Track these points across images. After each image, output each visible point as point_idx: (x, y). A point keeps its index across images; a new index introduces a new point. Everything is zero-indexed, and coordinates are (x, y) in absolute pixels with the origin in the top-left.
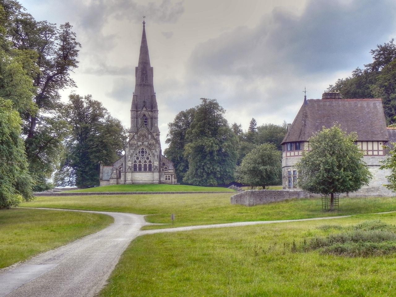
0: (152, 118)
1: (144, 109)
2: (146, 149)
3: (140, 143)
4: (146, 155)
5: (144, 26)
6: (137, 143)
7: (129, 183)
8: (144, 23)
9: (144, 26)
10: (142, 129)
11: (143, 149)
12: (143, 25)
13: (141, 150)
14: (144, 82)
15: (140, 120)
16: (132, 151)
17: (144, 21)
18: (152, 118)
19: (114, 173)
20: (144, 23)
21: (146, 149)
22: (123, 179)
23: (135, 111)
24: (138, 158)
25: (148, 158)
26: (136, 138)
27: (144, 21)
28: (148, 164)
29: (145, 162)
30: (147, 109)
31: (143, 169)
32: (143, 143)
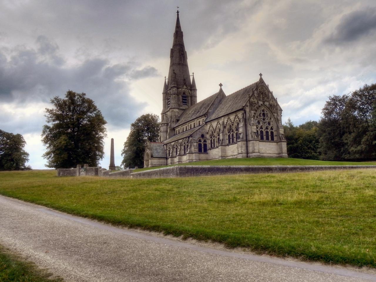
0: (191, 97)
1: (185, 87)
2: (267, 112)
3: (261, 103)
4: (267, 119)
5: (178, 15)
6: (258, 103)
7: (257, 155)
8: (178, 12)
9: (178, 15)
10: (261, 85)
11: (263, 111)
13: (262, 112)
14: (182, 62)
15: (181, 98)
16: (253, 112)
17: (178, 11)
18: (191, 97)
19: (194, 146)
20: (178, 12)
21: (267, 112)
22: (244, 150)
23: (174, 87)
24: (259, 122)
25: (269, 124)
26: (256, 95)
27: (178, 11)
28: (269, 131)
29: (267, 128)
30: (187, 87)
31: (265, 137)
32: (264, 102)
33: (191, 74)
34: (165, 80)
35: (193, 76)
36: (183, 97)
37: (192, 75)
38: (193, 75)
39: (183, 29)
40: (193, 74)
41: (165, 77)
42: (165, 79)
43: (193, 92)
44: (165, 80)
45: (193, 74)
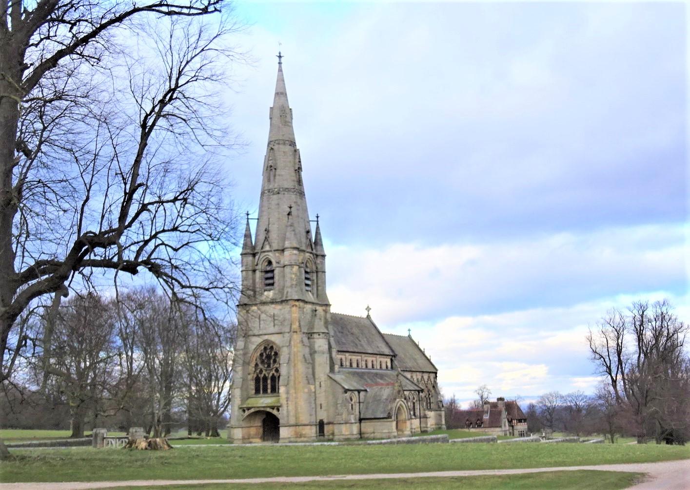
5: (280, 63)
8: (280, 57)
9: (280, 63)
12: (278, 61)
17: (280, 53)
20: (280, 57)
27: (280, 53)
33: (312, 217)
34: (248, 221)
35: (316, 223)
36: (306, 272)
37: (316, 219)
38: (317, 221)
39: (292, 103)
40: (318, 217)
41: (248, 214)
42: (248, 219)
43: (319, 260)
44: (248, 221)
45: (318, 217)
